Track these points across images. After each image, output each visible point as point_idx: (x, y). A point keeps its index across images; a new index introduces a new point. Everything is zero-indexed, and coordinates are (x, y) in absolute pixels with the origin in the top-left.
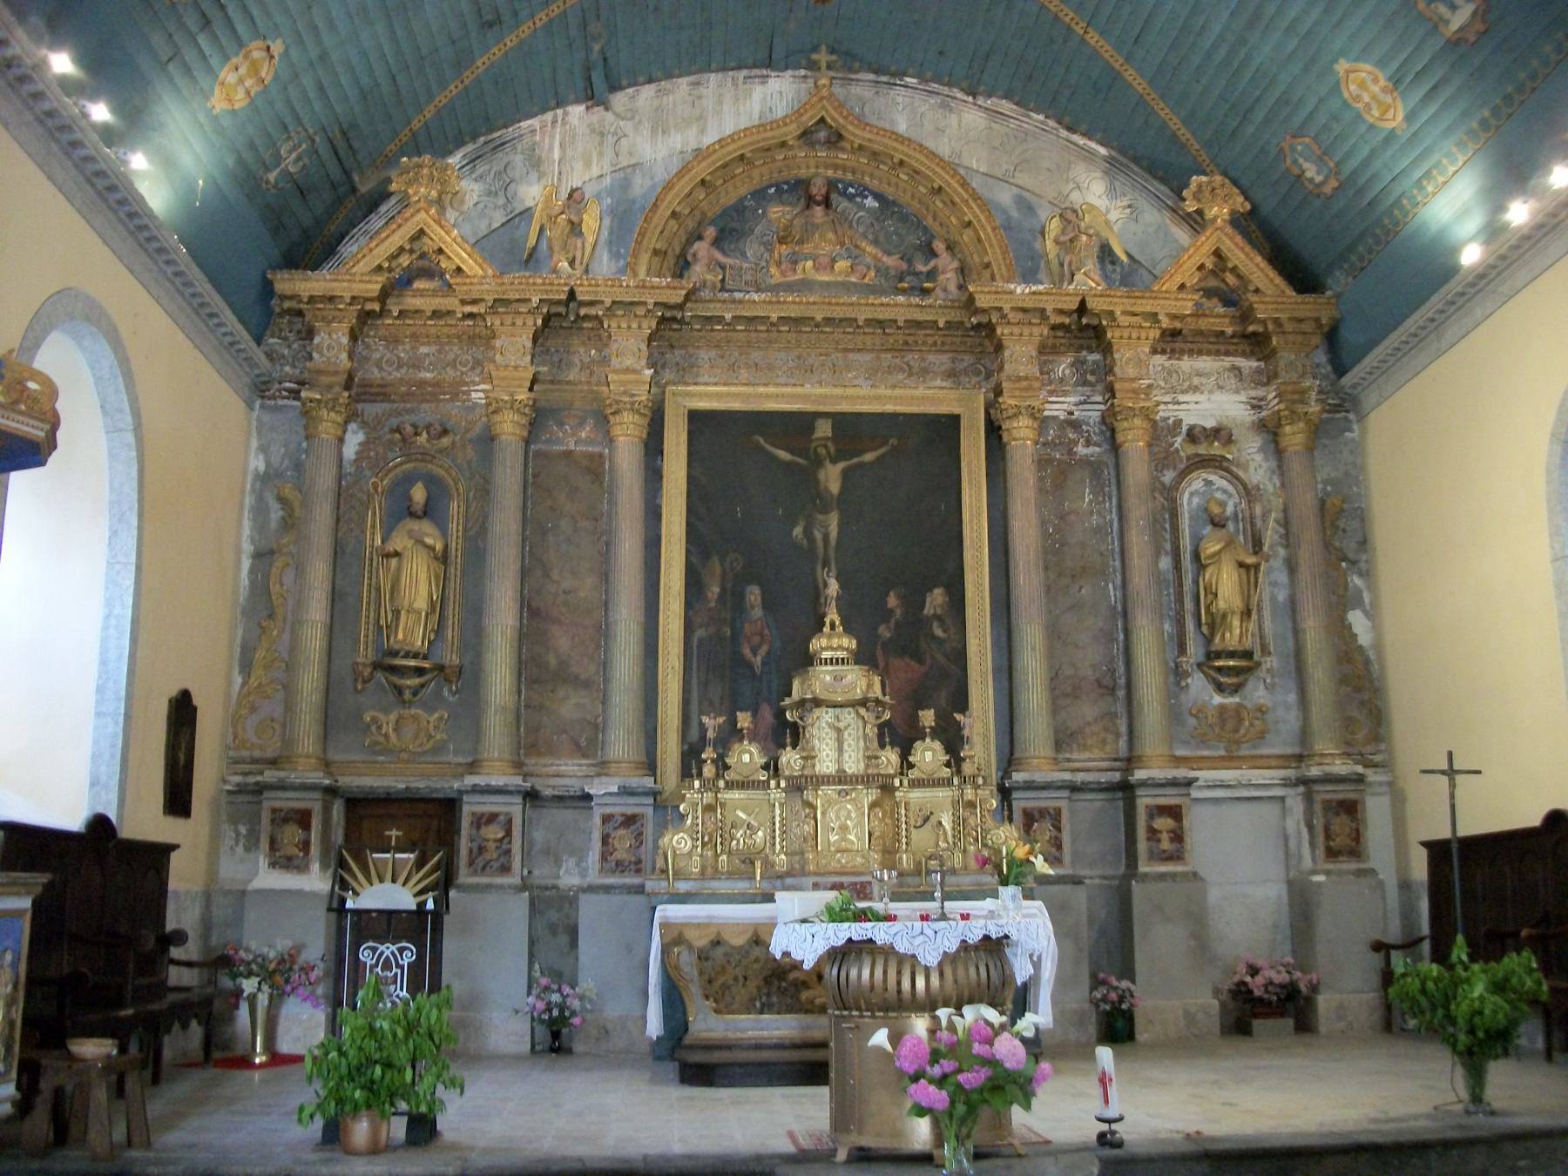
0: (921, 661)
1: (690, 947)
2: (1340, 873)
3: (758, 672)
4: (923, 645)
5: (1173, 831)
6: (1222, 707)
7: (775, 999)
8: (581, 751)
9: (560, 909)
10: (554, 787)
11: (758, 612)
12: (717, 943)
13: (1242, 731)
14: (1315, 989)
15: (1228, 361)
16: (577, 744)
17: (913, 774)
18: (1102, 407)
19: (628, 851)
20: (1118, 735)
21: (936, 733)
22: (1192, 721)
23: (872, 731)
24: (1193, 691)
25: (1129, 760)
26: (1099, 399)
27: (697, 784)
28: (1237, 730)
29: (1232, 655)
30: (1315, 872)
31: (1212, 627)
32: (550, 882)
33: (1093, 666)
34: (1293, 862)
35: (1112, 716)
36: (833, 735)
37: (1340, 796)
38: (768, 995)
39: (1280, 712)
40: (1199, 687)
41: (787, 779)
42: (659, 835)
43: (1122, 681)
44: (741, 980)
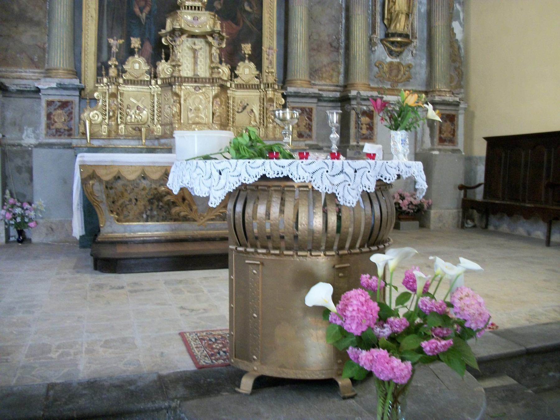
0: (237, 24)
1: (100, 181)
2: (446, 151)
3: (143, 23)
4: (239, 15)
5: (368, 124)
6: (391, 63)
7: (155, 213)
8: (34, 64)
9: (23, 158)
10: (17, 85)
12: (118, 178)
13: (400, 77)
14: (430, 207)
16: (32, 60)
17: (238, 81)
19: (63, 123)
20: (339, 73)
21: (251, 59)
22: (376, 69)
23: (215, 52)
24: (377, 53)
25: (345, 87)
27: (105, 80)
28: (397, 76)
29: (400, 35)
30: (433, 150)
31: (390, 20)
32: (16, 142)
33: (328, 36)
34: (419, 144)
35: (337, 62)
36: (191, 54)
37: (448, 112)
38: (151, 210)
39: (418, 69)
41: (162, 79)
42: (81, 111)
43: (343, 45)
44: (134, 201)
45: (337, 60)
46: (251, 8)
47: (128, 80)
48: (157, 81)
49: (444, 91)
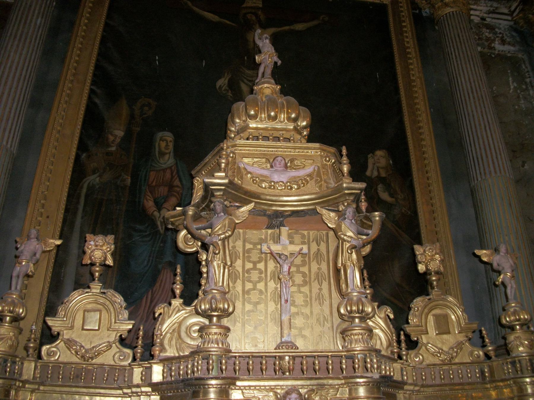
11: (168, 161)
18: (509, 18)
26: (506, 11)
46: (391, 195)
47: (57, 365)
48: (148, 371)
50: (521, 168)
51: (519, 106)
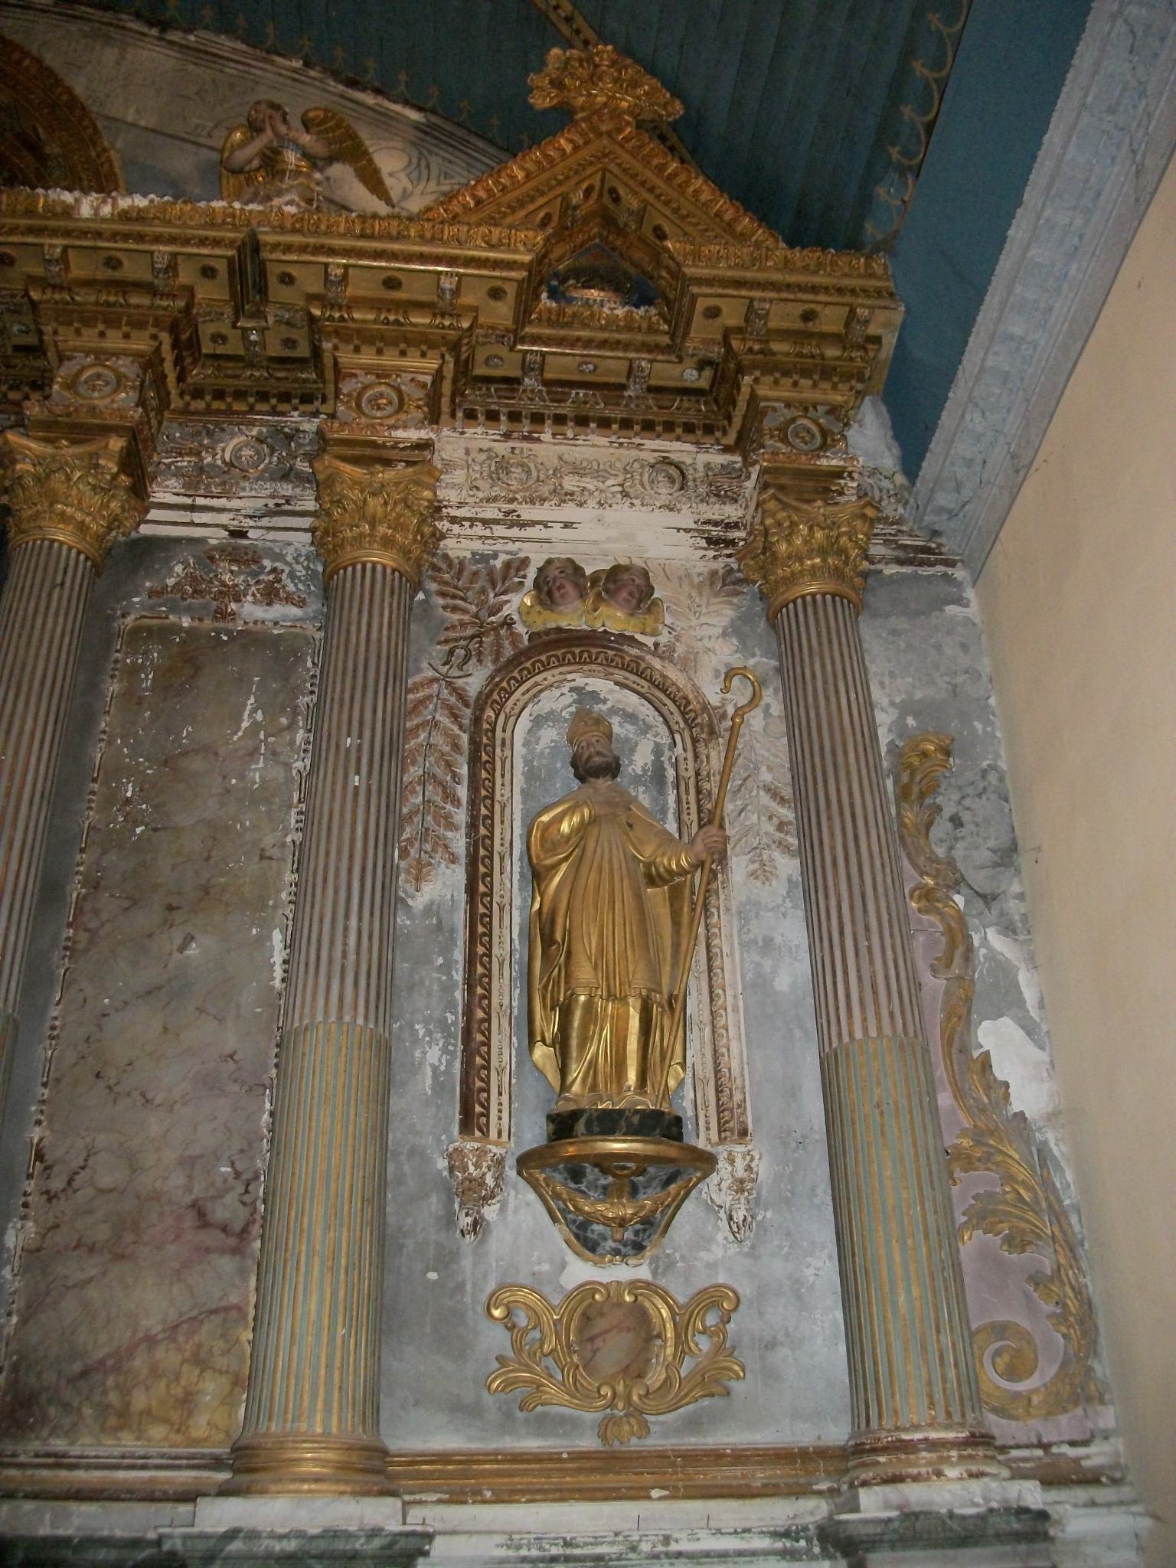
6: (587, 1290)
15: (654, 446)
24: (499, 1242)
33: (188, 1163)
40: (525, 1240)
45: (234, 1299)
49: (933, 1445)
50: (176, 956)
51: (241, 777)
